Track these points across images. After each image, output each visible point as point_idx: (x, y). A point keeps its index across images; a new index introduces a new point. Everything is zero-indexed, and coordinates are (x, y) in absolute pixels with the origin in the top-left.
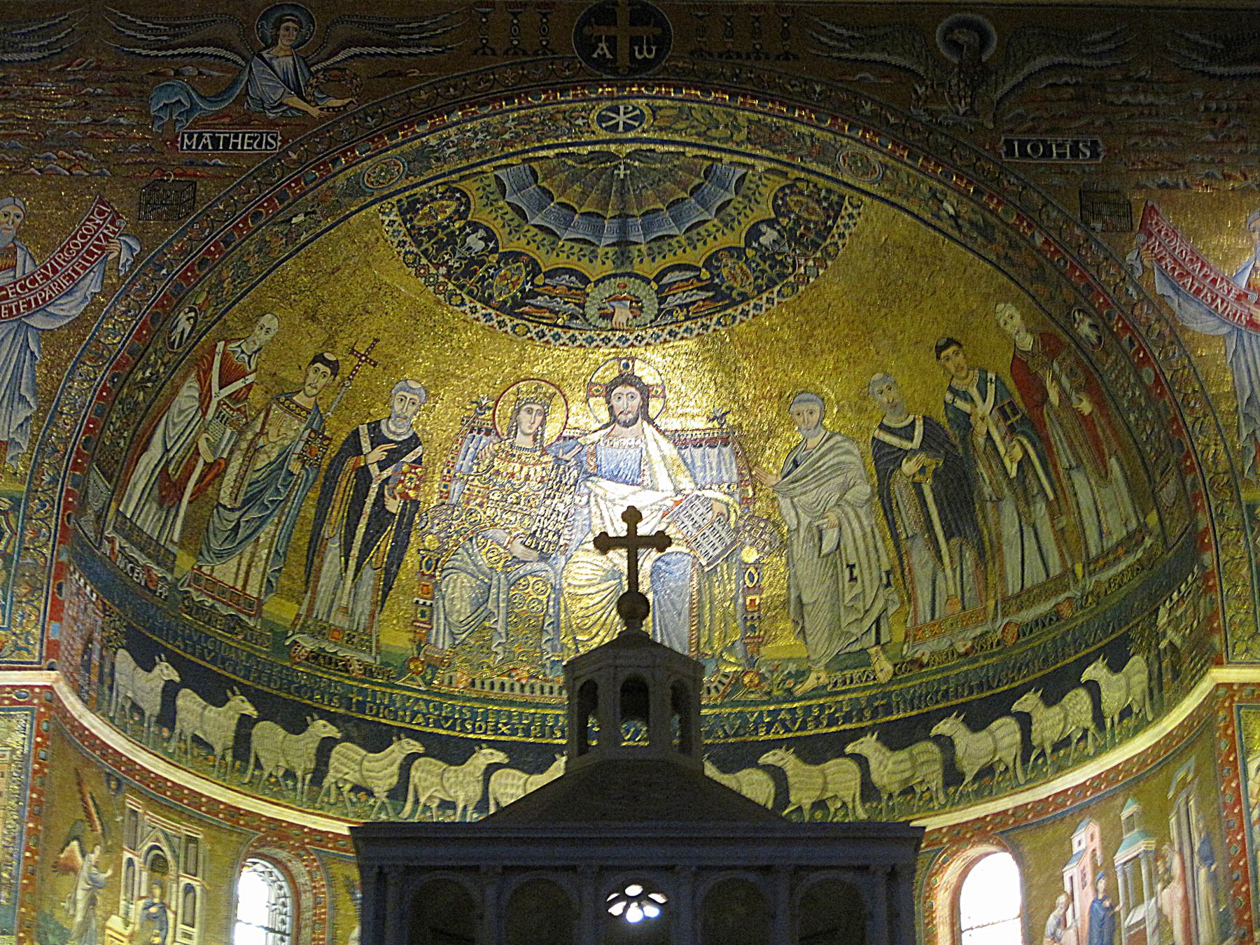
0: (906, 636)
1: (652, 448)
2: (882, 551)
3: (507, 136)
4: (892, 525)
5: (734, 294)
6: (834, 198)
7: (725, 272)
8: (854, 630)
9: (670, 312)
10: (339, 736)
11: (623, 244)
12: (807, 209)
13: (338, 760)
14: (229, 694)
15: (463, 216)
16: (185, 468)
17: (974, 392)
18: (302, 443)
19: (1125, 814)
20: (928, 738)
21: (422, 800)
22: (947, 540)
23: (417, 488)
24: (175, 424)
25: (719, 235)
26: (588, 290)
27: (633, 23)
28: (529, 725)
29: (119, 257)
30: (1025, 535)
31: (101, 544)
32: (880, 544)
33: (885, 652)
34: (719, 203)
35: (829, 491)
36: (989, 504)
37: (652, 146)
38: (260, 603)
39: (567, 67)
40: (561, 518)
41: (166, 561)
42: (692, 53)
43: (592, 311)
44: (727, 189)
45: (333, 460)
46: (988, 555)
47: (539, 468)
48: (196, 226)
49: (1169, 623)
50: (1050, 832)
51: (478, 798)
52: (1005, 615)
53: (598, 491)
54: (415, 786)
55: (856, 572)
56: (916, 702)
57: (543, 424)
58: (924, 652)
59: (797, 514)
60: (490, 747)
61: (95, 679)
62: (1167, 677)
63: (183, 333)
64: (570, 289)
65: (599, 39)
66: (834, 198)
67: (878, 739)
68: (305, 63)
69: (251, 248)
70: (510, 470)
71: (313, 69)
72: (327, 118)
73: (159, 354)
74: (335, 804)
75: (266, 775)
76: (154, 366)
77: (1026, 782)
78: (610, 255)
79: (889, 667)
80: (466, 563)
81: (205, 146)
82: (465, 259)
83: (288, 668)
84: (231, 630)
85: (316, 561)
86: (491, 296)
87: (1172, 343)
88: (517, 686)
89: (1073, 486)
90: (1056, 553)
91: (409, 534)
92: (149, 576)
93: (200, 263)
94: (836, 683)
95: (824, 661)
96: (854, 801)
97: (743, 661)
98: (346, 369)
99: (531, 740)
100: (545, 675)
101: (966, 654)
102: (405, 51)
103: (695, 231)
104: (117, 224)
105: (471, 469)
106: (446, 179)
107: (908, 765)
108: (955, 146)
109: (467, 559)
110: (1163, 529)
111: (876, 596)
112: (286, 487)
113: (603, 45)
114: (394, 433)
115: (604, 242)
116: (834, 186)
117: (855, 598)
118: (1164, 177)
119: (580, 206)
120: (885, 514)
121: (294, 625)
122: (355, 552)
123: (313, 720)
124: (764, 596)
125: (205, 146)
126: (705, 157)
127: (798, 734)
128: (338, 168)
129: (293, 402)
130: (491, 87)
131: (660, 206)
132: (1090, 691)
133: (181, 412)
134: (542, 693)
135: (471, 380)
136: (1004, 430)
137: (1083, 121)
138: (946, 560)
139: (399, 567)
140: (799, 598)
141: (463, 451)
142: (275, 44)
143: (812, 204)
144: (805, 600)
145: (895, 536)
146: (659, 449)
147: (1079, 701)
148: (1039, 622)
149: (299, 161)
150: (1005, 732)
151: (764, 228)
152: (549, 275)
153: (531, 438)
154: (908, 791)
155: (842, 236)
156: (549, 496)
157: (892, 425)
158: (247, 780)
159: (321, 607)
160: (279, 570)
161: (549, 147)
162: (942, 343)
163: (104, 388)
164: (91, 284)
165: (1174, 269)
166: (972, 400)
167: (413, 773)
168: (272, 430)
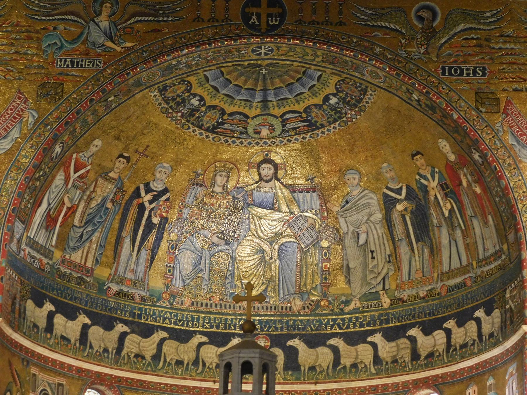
0: (397, 286)
1: (279, 192)
2: (387, 245)
3: (209, 58)
4: (391, 234)
5: (318, 124)
6: (363, 87)
7: (313, 115)
8: (373, 282)
9: (288, 131)
10: (129, 331)
11: (265, 102)
12: (351, 90)
13: (128, 342)
14: (78, 314)
15: (189, 91)
16: (58, 211)
17: (429, 176)
18: (112, 194)
19: (489, 383)
20: (405, 337)
21: (168, 360)
22: (417, 243)
23: (167, 212)
24: (53, 192)
25: (310, 99)
27: (269, 6)
28: (219, 324)
29: (27, 121)
30: (452, 244)
31: (19, 253)
32: (386, 242)
33: (387, 294)
34: (310, 85)
36: (435, 228)
37: (278, 61)
38: (93, 270)
39: (237, 29)
40: (236, 225)
41: (48, 254)
42: (296, 22)
43: (250, 130)
45: (127, 201)
46: (435, 251)
47: (225, 202)
48: (64, 105)
49: (510, 297)
50: (457, 387)
51: (194, 358)
52: (442, 281)
53: (253, 212)
54: (165, 354)
55: (375, 254)
56: (400, 319)
57: (227, 181)
58: (405, 295)
60: (200, 334)
61: (17, 316)
62: (508, 323)
64: (240, 121)
65: (252, 14)
67: (382, 336)
68: (115, 24)
69: (89, 114)
70: (211, 202)
71: (118, 27)
72: (124, 52)
73: (46, 164)
74: (125, 364)
77: (449, 362)
78: (259, 106)
79: (388, 301)
80: (190, 246)
81: (68, 66)
82: (190, 109)
83: (105, 300)
84: (79, 284)
85: (119, 248)
86: (202, 125)
87: (514, 168)
88: (214, 305)
89: (473, 224)
90: (465, 254)
91: (163, 233)
92: (41, 263)
93: (65, 123)
94: (364, 307)
95: (359, 296)
96: (370, 365)
98: (134, 159)
99: (220, 331)
101: (424, 298)
102: (161, 19)
104: (27, 103)
105: (193, 202)
106: (180, 77)
107: (396, 349)
108: (418, 70)
109: (190, 244)
110: (509, 252)
112: (105, 215)
113: (254, 17)
114: (156, 187)
115: (256, 100)
116: (363, 82)
117: (374, 267)
118: (515, 86)
119: (245, 85)
120: (389, 228)
121: (108, 279)
122: (137, 243)
123: (117, 324)
124: (331, 263)
125: (68, 66)
126: (303, 67)
128: (129, 77)
129: (109, 176)
130: (201, 38)
131: (282, 85)
134: (225, 308)
136: (443, 194)
137: (480, 57)
138: (416, 252)
139: (158, 249)
141: (189, 194)
142: (100, 14)
143: (353, 88)
144: (350, 266)
145: (393, 239)
146: (282, 192)
147: (472, 326)
148: (457, 287)
149: (111, 74)
150: (439, 336)
151: (331, 97)
152: (231, 114)
153: (221, 188)
154: (395, 361)
157: (392, 187)
158: (86, 354)
159: (121, 270)
160: (102, 254)
161: (229, 62)
162: (414, 152)
163: (22, 184)
164: (15, 133)
165: (518, 132)
167: (164, 347)
168: (98, 190)
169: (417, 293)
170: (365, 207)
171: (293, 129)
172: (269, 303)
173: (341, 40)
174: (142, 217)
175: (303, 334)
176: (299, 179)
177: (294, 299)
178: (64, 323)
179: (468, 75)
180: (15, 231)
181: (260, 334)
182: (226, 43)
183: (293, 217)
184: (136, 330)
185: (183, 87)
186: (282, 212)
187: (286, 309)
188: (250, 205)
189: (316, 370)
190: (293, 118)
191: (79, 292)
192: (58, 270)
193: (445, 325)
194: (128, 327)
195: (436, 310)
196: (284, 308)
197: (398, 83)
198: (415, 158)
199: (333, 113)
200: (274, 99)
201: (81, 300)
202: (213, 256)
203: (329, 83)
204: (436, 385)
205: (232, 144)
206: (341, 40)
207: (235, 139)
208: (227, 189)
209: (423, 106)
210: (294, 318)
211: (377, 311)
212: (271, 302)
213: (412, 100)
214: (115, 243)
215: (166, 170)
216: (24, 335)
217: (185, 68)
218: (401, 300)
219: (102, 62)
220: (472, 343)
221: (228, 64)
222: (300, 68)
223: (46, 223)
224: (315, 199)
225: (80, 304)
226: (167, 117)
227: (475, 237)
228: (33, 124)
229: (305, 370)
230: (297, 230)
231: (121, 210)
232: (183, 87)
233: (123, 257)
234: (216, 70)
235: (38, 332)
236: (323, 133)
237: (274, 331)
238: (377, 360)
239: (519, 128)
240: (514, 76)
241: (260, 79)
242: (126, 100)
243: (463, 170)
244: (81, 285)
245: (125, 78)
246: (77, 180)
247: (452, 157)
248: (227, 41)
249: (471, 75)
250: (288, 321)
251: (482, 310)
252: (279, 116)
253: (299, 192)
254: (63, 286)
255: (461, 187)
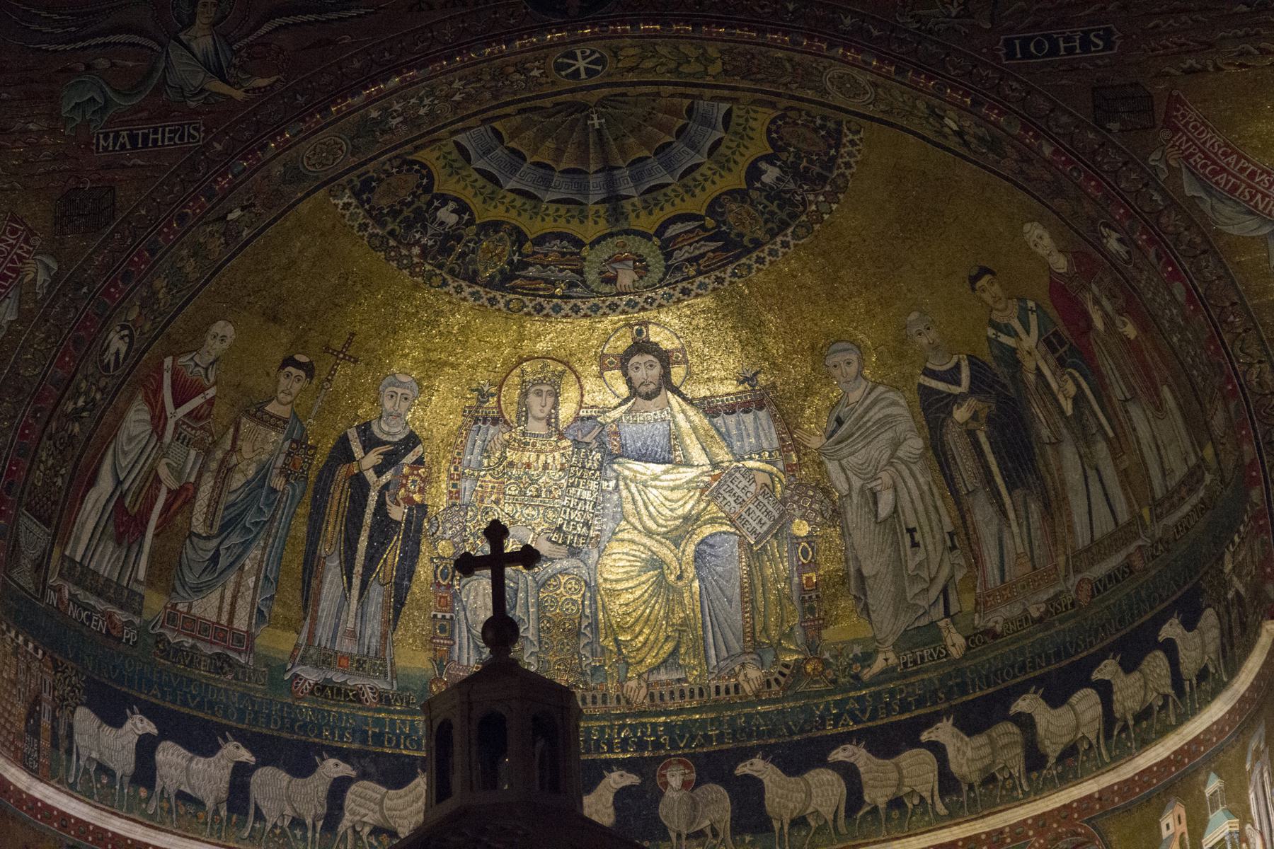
0: (977, 603)
1: (680, 418)
2: (943, 510)
3: (457, 97)
4: (950, 482)
5: (746, 241)
6: (831, 125)
7: (731, 220)
9: (679, 268)
10: (353, 774)
11: (614, 200)
14: (220, 741)
16: (146, 498)
17: (1016, 324)
18: (282, 457)
19: (1208, 791)
23: (422, 491)
24: (125, 454)
26: (584, 254)
29: (35, 280)
30: (1089, 480)
32: (939, 503)
34: (709, 144)
35: (878, 450)
36: (1048, 448)
39: (512, 15)
40: (589, 507)
43: (592, 276)
44: (714, 128)
45: (321, 472)
46: (1054, 505)
47: (557, 455)
48: (117, 236)
52: (1077, 571)
53: (627, 473)
55: (918, 536)
57: (555, 406)
58: (996, 620)
59: (847, 478)
61: (45, 744)
63: (117, 353)
64: (563, 255)
66: (831, 125)
67: (954, 725)
69: (185, 252)
70: (525, 460)
71: (235, 47)
73: (91, 379)
75: (269, 826)
76: (87, 393)
77: (1113, 759)
78: (602, 212)
79: (960, 640)
81: (123, 147)
83: (289, 706)
85: (314, 583)
86: (475, 272)
87: (1204, 252)
89: (1130, 420)
90: (1122, 497)
91: (418, 543)
94: (905, 664)
95: (891, 640)
97: (804, 647)
98: (322, 371)
100: (586, 683)
101: (1040, 620)
102: (333, 16)
103: (689, 177)
104: (32, 241)
106: (398, 151)
107: (988, 750)
108: (948, 55)
110: (1219, 463)
111: (941, 560)
112: (269, 506)
114: (388, 434)
115: (594, 198)
116: (828, 112)
117: (920, 565)
119: (557, 161)
120: (942, 469)
121: (293, 656)
122: (358, 569)
123: (323, 760)
125: (123, 147)
127: (870, 724)
130: (429, 48)
131: (646, 153)
132: (1165, 651)
133: (130, 439)
135: (469, 366)
136: (1052, 361)
138: (1012, 515)
139: (410, 580)
140: (859, 571)
141: (469, 444)
142: (192, 23)
144: (865, 572)
145: (955, 492)
146: (686, 419)
147: (1157, 664)
148: (1112, 578)
150: (1086, 704)
151: (763, 166)
152: (541, 240)
153: (544, 423)
154: (990, 780)
155: (848, 165)
156: (572, 485)
157: (937, 368)
158: (246, 834)
159: (323, 634)
160: (272, 597)
161: (508, 104)
162: (974, 273)
165: (1204, 166)
166: (1017, 334)
168: (246, 447)
169: (1025, 610)
170: (882, 426)
171: (690, 261)
172: (685, 680)
173: (760, 11)
174: (364, 505)
175: (771, 744)
176: (721, 380)
177: (743, 665)
178: (184, 763)
179: (1070, 51)
180: (22, 540)
181: (670, 756)
182: (488, 50)
183: (719, 476)
184: (372, 769)
185: (412, 179)
186: (692, 466)
187: (727, 691)
188: (618, 456)
189: (808, 825)
190: (686, 232)
191: (219, 690)
192: (160, 638)
193: (1096, 676)
194: (352, 765)
195: (1071, 643)
196: (722, 689)
197: (906, 97)
198: (979, 284)
199: (774, 207)
200: (631, 191)
201: (227, 707)
202: (543, 585)
203: (753, 130)
204: (1088, 821)
205: (554, 314)
206: (760, 11)
207: (559, 301)
208: (557, 425)
209: (974, 143)
210: (746, 710)
211: (936, 668)
212: (690, 680)
213: (945, 137)
214: (304, 570)
215: (407, 391)
216: (71, 790)
217: (404, 128)
218: (992, 634)
219: (203, 128)
220: (1160, 703)
221: (508, 110)
222: (676, 100)
223: (117, 526)
224: (766, 427)
225: (225, 716)
226: (388, 259)
227: (1141, 450)
228: (50, 285)
229: (782, 828)
230: (733, 504)
231: (310, 492)
232: (412, 179)
233: (327, 604)
234: (482, 128)
235: (111, 785)
236: (760, 260)
237: (702, 746)
238: (948, 782)
239: (1207, 157)
240: (1183, 40)
241: (591, 141)
242: (275, 220)
243: (1090, 290)
244: (225, 674)
245: (259, 159)
246: (184, 423)
247: (1061, 263)
248: (489, 45)
249: (1078, 51)
250: (733, 719)
251: (1175, 621)
252: (652, 232)
253: (727, 413)
254: (176, 676)
255: (1092, 335)
